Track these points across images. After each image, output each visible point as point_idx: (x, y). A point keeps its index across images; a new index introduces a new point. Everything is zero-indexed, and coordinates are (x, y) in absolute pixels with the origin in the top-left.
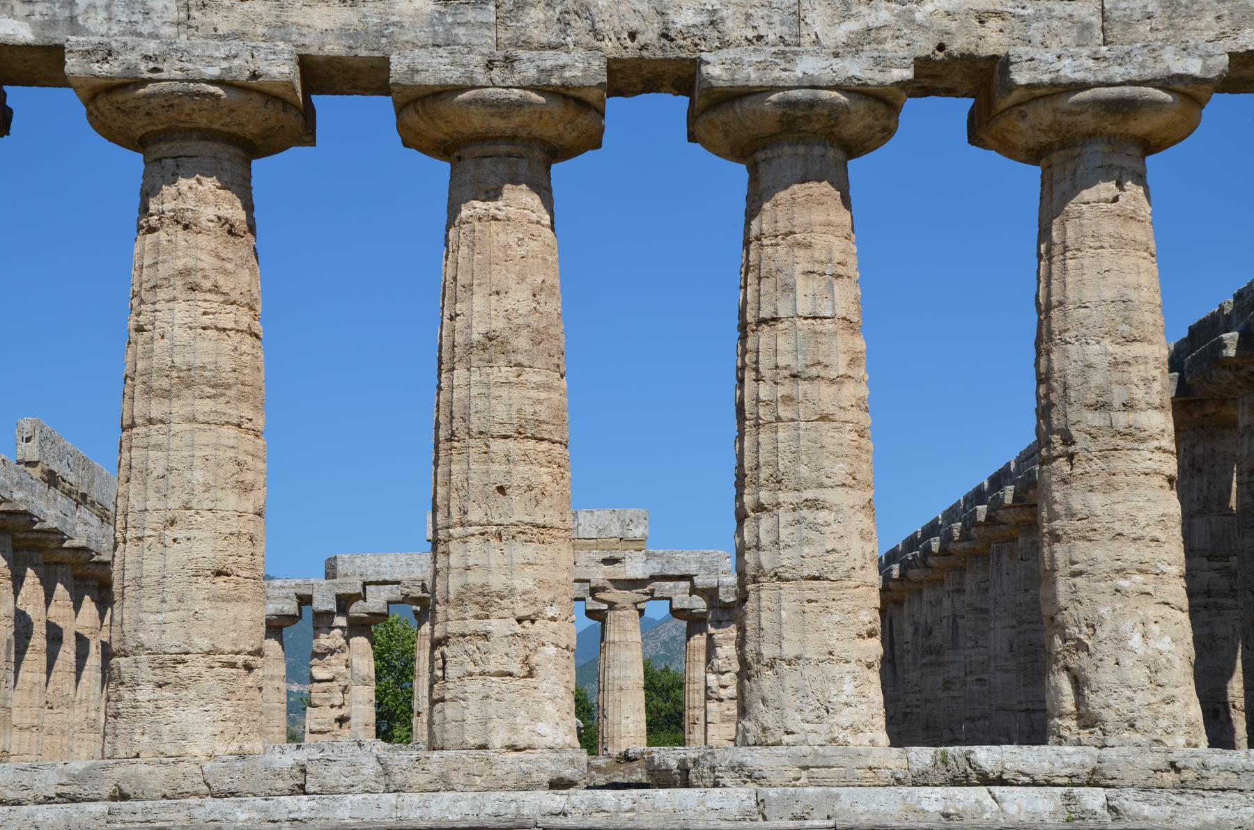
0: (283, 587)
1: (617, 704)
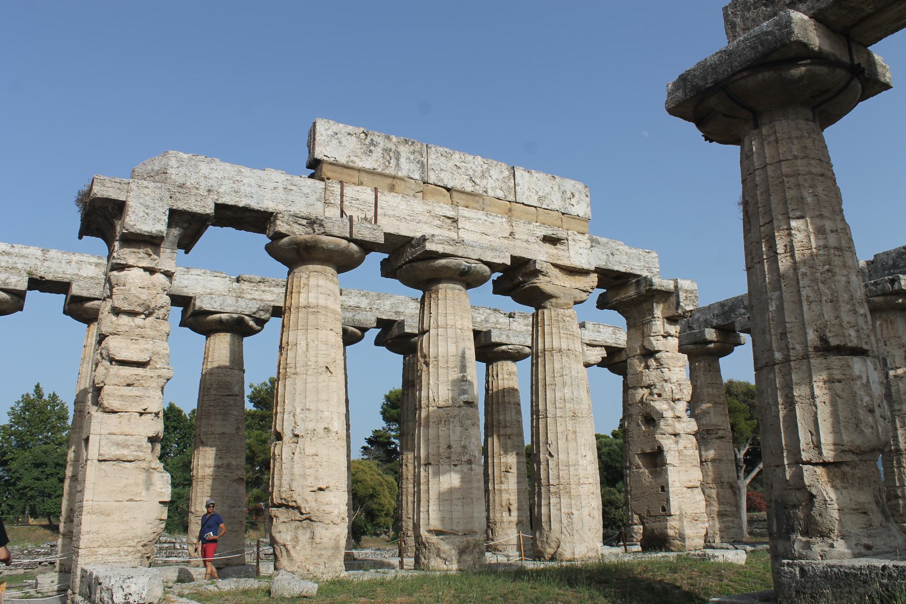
0: (9, 254)
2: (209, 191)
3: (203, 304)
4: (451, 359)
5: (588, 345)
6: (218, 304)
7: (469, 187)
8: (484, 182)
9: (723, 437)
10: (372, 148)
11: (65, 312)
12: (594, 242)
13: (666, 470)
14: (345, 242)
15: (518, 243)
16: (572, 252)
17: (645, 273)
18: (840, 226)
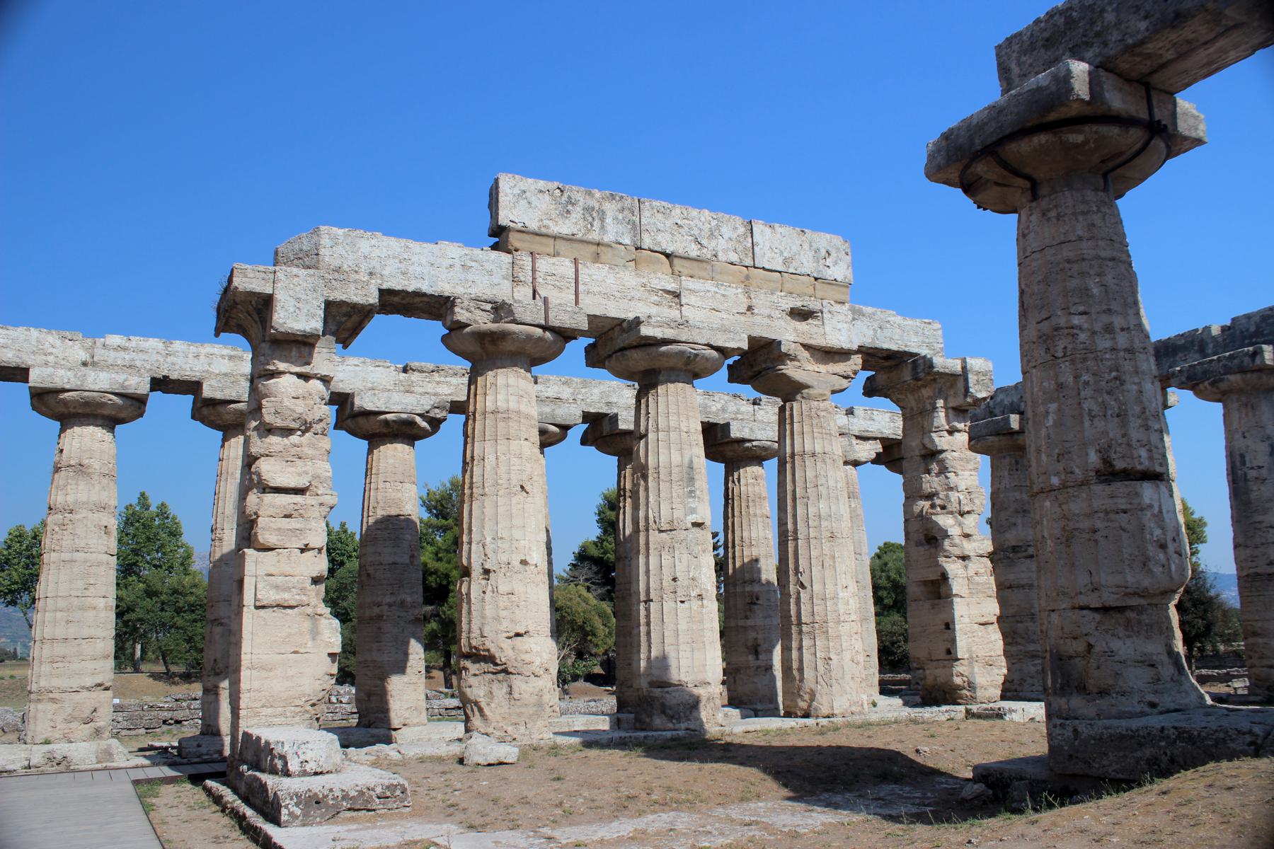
0: (125, 349)
1: (828, 562)
2: (371, 274)
3: (364, 402)
4: (675, 470)
5: (858, 437)
6: (382, 401)
7: (694, 251)
8: (713, 243)
9: (1032, 556)
10: (570, 207)
11: (193, 417)
12: (857, 314)
13: (952, 603)
14: (539, 331)
15: (758, 319)
16: (828, 328)
17: (924, 351)
18: (1133, 321)
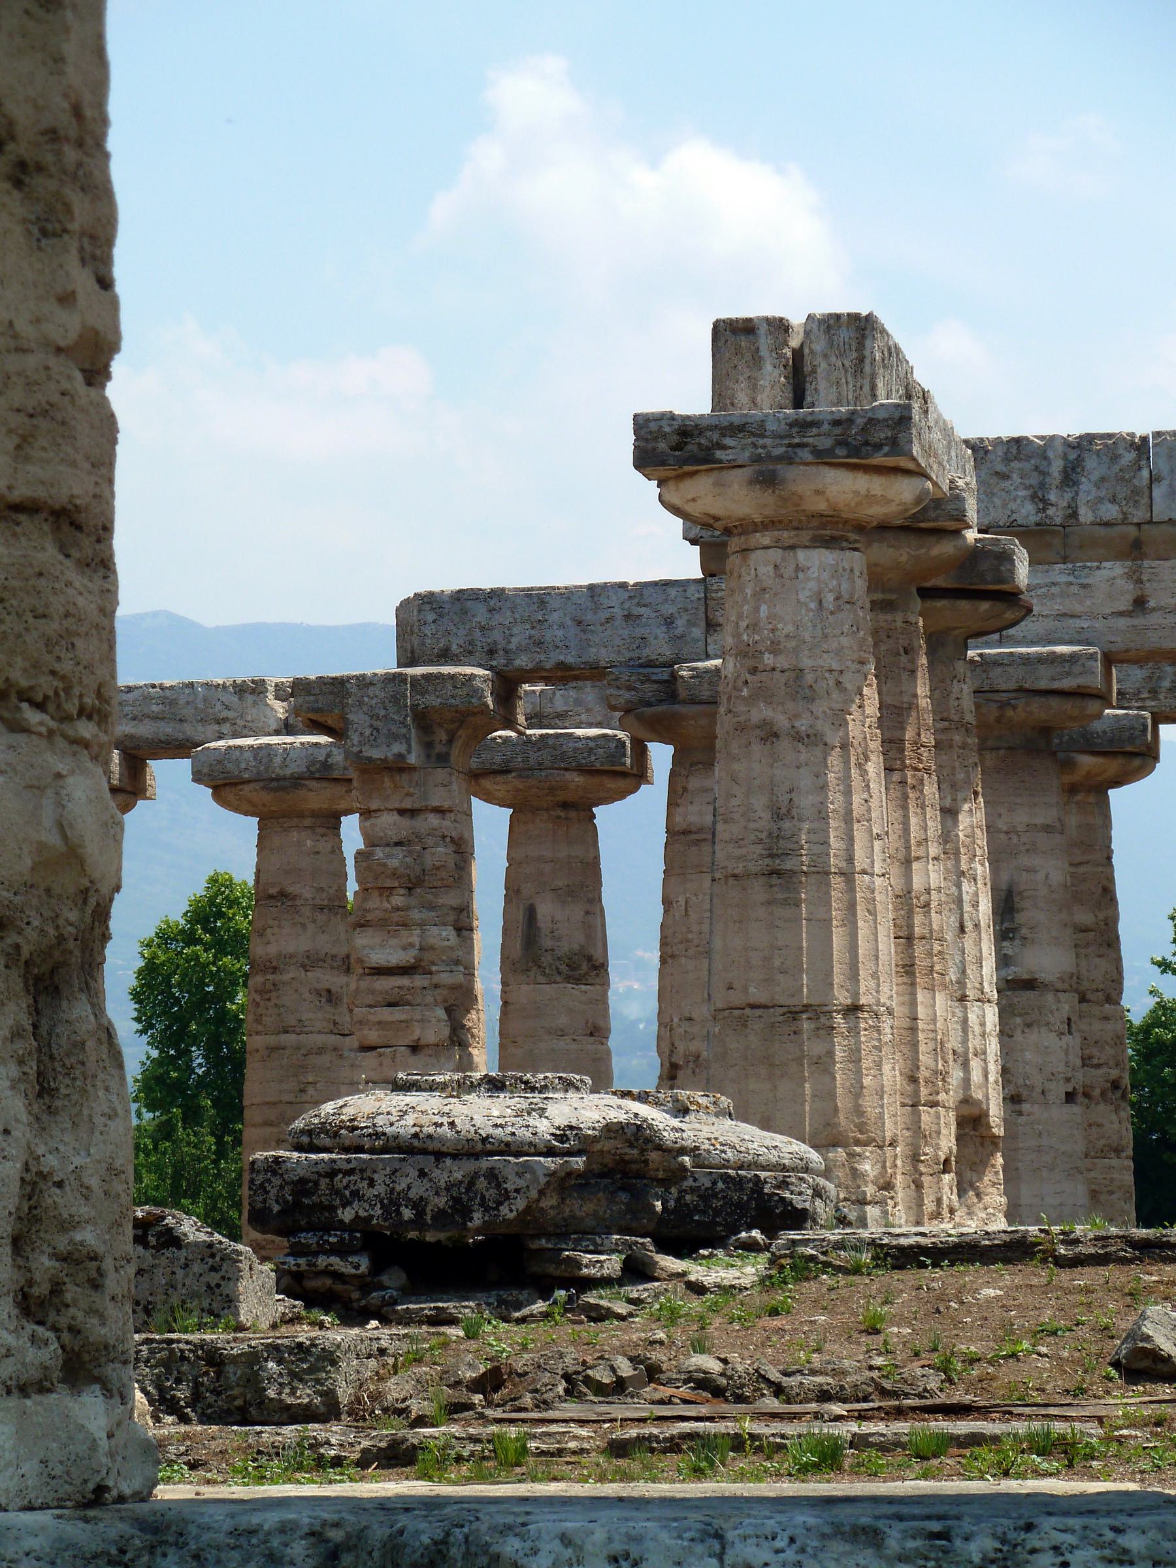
15: (1155, 619)
